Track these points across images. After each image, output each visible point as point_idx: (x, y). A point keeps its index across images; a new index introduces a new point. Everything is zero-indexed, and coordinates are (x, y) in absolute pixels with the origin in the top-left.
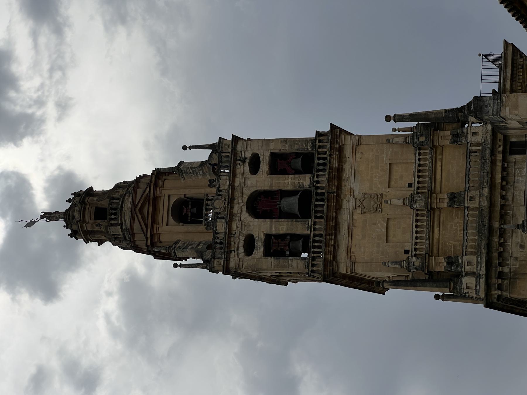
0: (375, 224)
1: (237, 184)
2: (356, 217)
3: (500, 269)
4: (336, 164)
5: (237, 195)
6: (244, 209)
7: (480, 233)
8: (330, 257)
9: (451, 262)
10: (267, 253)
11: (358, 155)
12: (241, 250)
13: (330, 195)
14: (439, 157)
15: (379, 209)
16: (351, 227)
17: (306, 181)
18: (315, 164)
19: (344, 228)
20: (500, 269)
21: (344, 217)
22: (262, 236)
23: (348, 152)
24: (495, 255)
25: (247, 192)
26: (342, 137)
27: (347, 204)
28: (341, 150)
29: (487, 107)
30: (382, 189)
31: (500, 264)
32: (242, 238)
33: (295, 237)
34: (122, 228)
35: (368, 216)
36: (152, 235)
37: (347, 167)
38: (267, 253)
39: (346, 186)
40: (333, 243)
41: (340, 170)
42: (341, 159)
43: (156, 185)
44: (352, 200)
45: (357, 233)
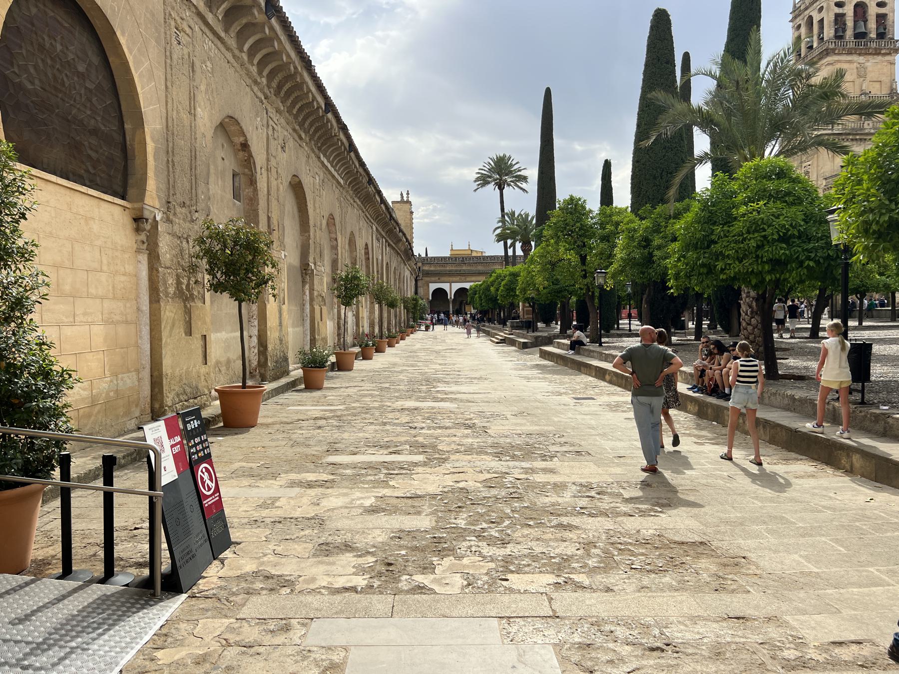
4: (883, 52)
7: (853, 129)
8: (837, 52)
15: (859, 76)
16: (850, 62)
17: (873, 35)
19: (849, 58)
21: (855, 58)
23: (888, 58)
27: (861, 59)
28: (890, 54)
30: (868, 79)
35: (855, 70)
37: (880, 57)
39: (870, 58)
41: (879, 54)
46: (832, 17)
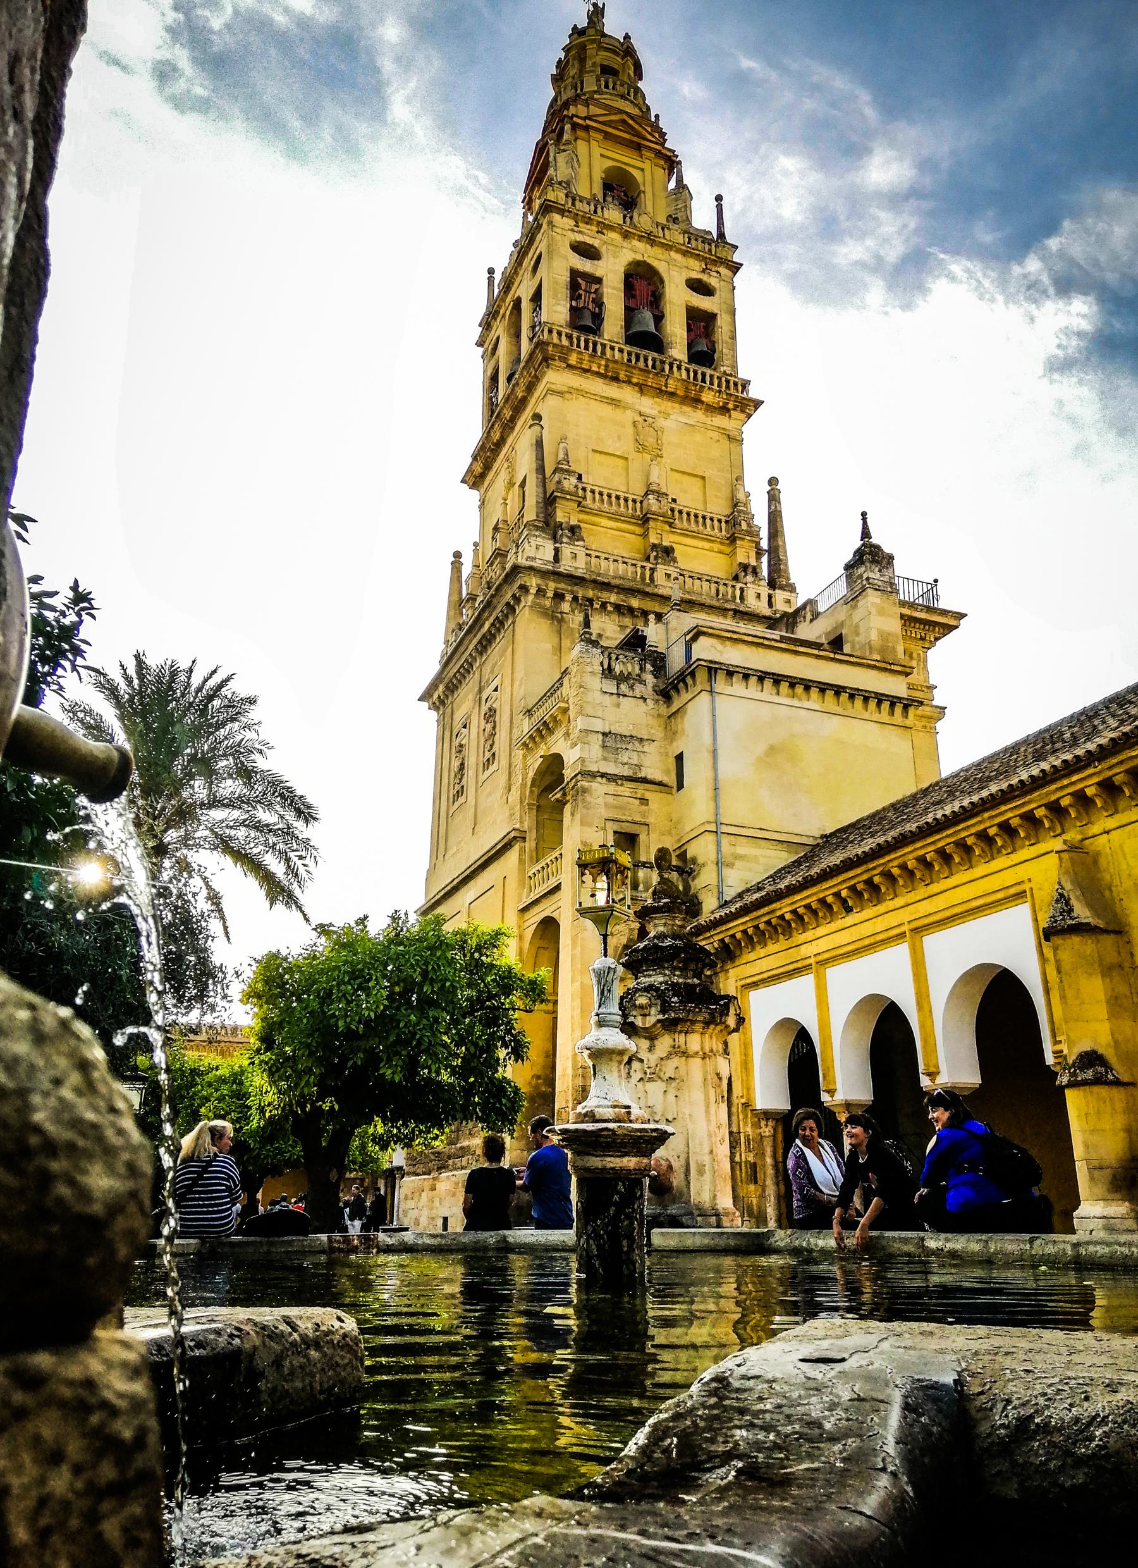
0: (619, 438)
1: (672, 253)
2: (628, 412)
3: (569, 597)
5: (657, 251)
6: (639, 258)
9: (574, 531)
10: (575, 274)
11: (716, 435)
12: (580, 238)
13: (663, 380)
14: (716, 546)
16: (614, 402)
18: (704, 369)
20: (569, 597)
22: (598, 274)
24: (590, 594)
25: (661, 267)
26: (743, 416)
27: (648, 404)
28: (724, 410)
29: (880, 571)
31: (575, 599)
32: (596, 243)
33: (598, 318)
34: (595, 92)
36: (587, 128)
38: (575, 274)
40: (595, 368)
42: (710, 409)
43: (658, 154)
44: (654, 412)
45: (607, 410)
46: (565, 277)
